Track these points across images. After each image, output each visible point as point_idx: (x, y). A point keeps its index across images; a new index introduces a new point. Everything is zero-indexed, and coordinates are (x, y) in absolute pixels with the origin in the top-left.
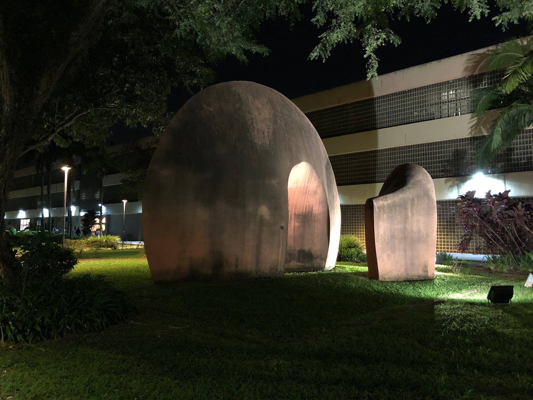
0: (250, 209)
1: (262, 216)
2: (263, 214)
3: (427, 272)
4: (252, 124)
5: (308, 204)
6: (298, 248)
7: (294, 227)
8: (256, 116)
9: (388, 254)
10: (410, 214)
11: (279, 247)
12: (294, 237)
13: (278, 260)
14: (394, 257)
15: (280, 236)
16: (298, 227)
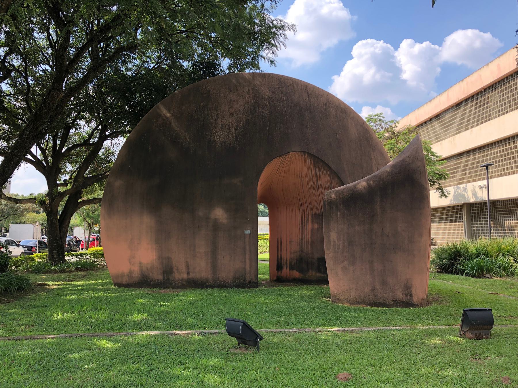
0: (201, 213)
1: (216, 220)
2: (217, 217)
3: (411, 295)
4: (216, 120)
8: (224, 111)
11: (245, 254)
12: (312, 242)
13: (245, 269)
15: (245, 242)
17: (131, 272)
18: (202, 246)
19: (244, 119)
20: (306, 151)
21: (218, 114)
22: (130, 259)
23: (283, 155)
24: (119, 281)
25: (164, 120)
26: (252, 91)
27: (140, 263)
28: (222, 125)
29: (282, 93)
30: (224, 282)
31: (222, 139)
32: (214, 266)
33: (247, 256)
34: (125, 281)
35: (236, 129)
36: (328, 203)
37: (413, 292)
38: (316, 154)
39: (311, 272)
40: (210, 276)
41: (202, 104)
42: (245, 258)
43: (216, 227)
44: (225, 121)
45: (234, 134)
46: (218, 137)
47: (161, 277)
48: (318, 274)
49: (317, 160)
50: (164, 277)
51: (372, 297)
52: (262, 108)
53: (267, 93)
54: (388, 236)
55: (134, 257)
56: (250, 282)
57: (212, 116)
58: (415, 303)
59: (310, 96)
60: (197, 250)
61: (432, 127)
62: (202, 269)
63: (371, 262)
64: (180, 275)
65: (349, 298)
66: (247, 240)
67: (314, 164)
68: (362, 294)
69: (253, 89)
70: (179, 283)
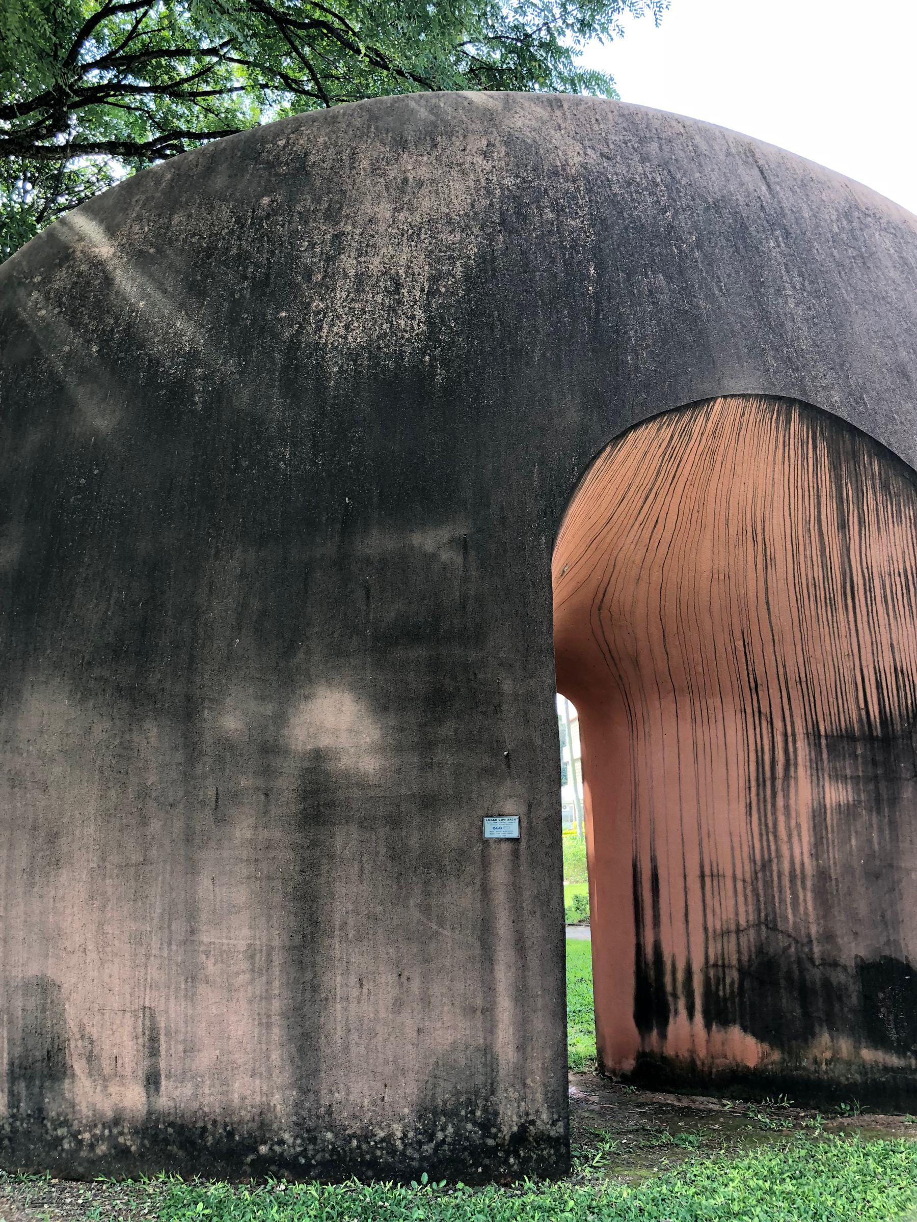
0: (232, 718)
1: (318, 756)
2: (325, 741)
5: (887, 662)
6: (854, 949)
7: (819, 814)
11: (488, 959)
12: (823, 875)
13: (487, 1051)
15: (485, 891)
16: (848, 812)
18: (238, 920)
19: (473, 251)
21: (338, 236)
25: (80, 274)
28: (360, 280)
29: (644, 159)
30: (367, 1136)
31: (356, 337)
33: (504, 977)
35: (431, 293)
39: (825, 1038)
41: (266, 200)
42: (489, 989)
43: (319, 800)
44: (376, 261)
45: (419, 314)
46: (339, 328)
48: (868, 1055)
52: (557, 209)
56: (520, 1138)
57: (312, 245)
59: (772, 179)
60: (206, 937)
66: (500, 874)
67: (835, 467)
69: (506, 143)
70: (97, 1139)
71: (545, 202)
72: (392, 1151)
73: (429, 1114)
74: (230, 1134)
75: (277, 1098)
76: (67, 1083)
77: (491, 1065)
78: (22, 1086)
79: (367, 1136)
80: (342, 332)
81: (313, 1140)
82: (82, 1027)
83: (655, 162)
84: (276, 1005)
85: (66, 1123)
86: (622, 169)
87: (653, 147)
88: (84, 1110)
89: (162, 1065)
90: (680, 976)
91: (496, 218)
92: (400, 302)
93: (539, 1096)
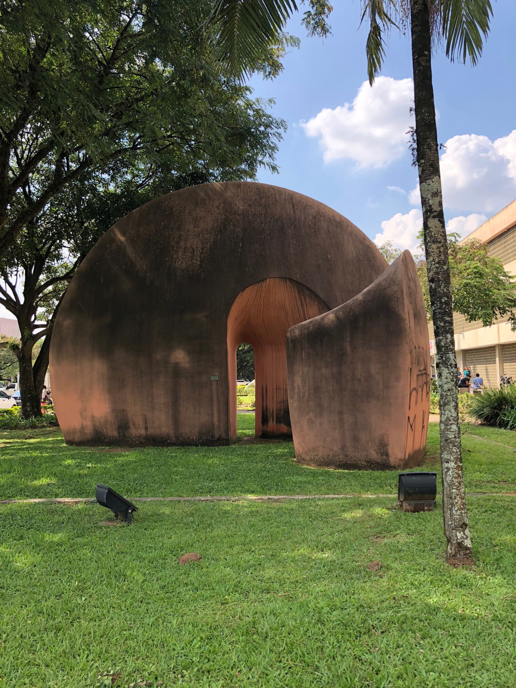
1: (177, 364)
2: (178, 361)
3: (387, 455)
9: (310, 419)
10: (349, 348)
14: (321, 424)
15: (211, 391)
17: (83, 428)
18: (161, 397)
19: (212, 240)
20: (287, 276)
22: (81, 412)
23: (258, 282)
24: (71, 438)
25: (118, 245)
26: (223, 205)
27: (93, 417)
28: (185, 248)
29: (260, 205)
30: (189, 439)
31: (184, 266)
32: (176, 421)
34: (77, 437)
35: (201, 253)
36: (292, 340)
37: (390, 451)
38: (299, 280)
40: (171, 432)
43: (177, 372)
45: (198, 259)
46: (180, 263)
47: (115, 434)
49: (302, 288)
50: (119, 433)
51: (342, 457)
52: (234, 226)
53: (240, 206)
54: (360, 380)
55: (85, 410)
56: (219, 439)
57: (174, 238)
58: (392, 464)
61: (510, 239)
62: (162, 423)
63: (341, 413)
64: (137, 431)
65: (317, 458)
68: (331, 453)
69: (224, 203)
71: (231, 224)
72: (194, 441)
73: (201, 434)
74: (162, 439)
75: (171, 432)
76: (129, 430)
77: (213, 424)
78: (120, 431)
79: (189, 439)
80: (181, 264)
81: (178, 439)
82: (132, 419)
83: (263, 206)
84: (170, 413)
85: (130, 437)
86: (253, 210)
87: (264, 200)
88: (133, 434)
89: (148, 426)
90: (271, 412)
91: (218, 230)
92: (194, 256)
93: (223, 431)
